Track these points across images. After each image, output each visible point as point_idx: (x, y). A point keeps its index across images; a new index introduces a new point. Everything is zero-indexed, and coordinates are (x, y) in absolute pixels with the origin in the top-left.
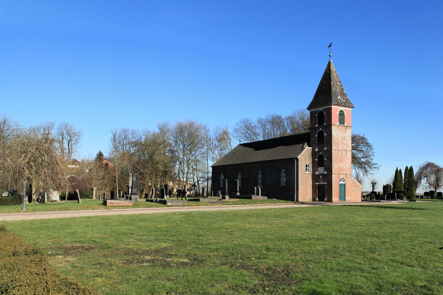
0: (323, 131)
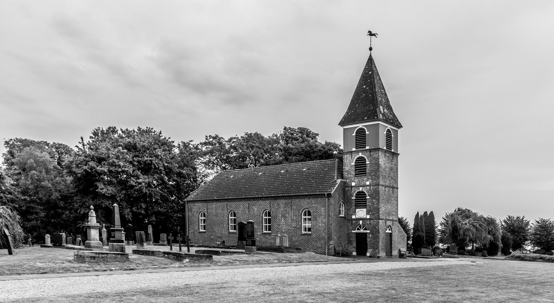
0: (365, 157)
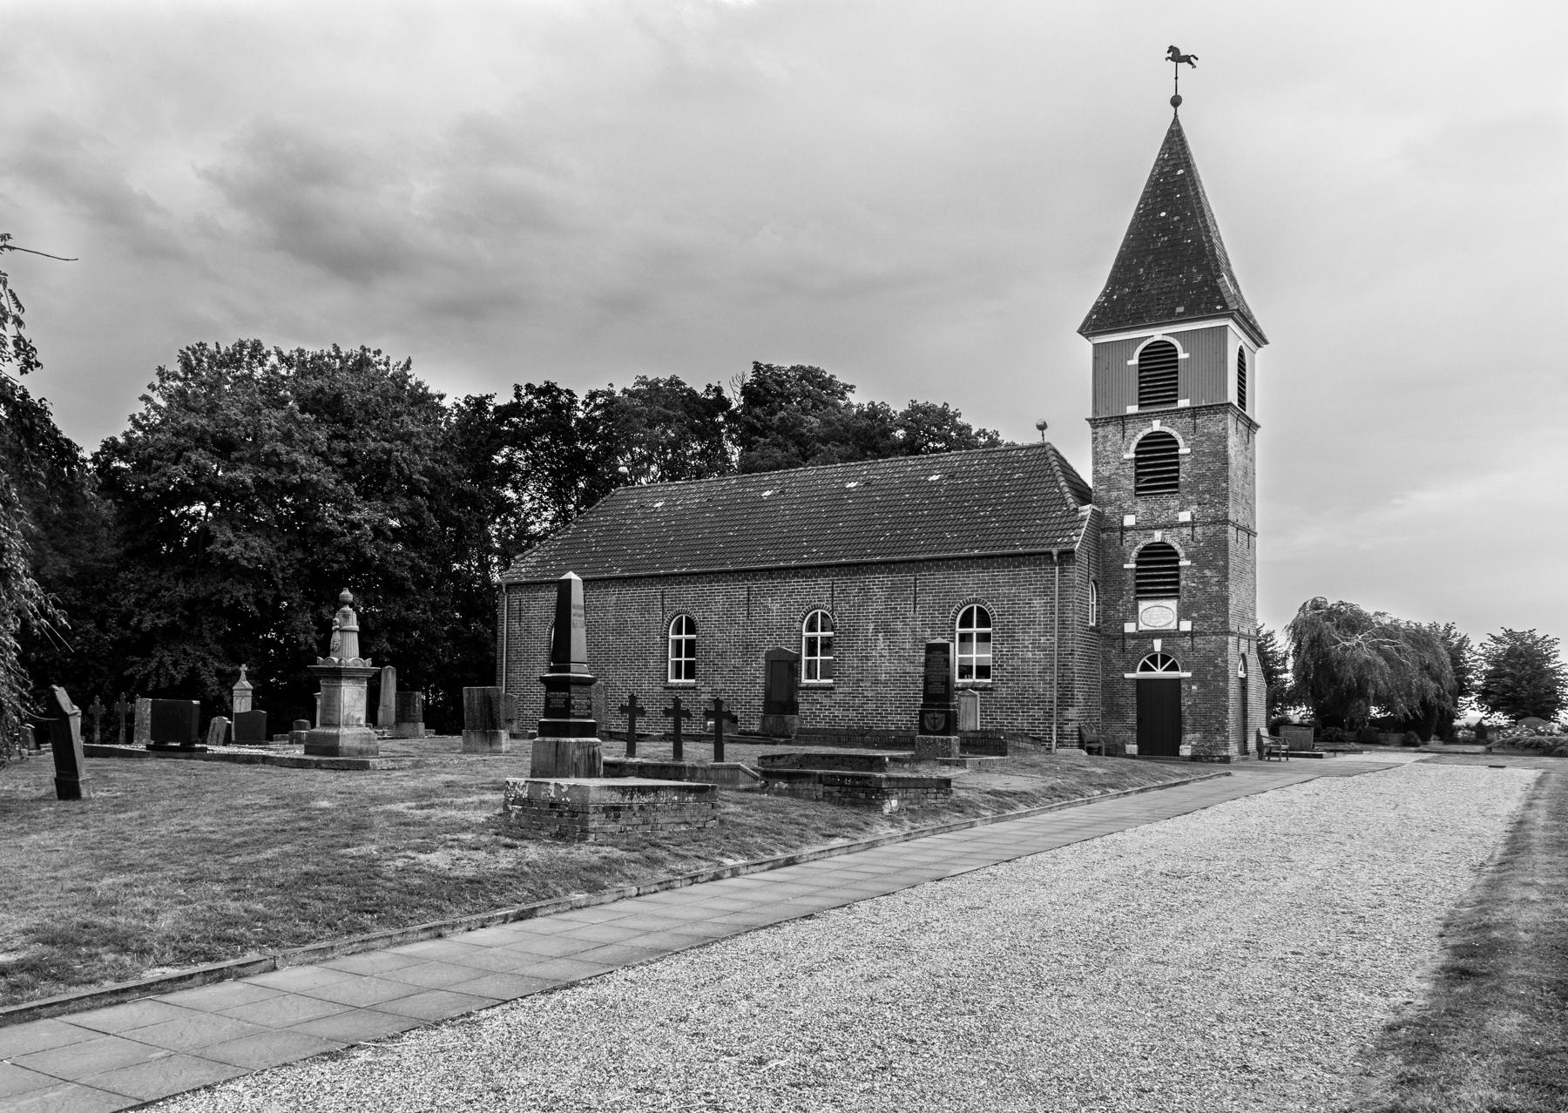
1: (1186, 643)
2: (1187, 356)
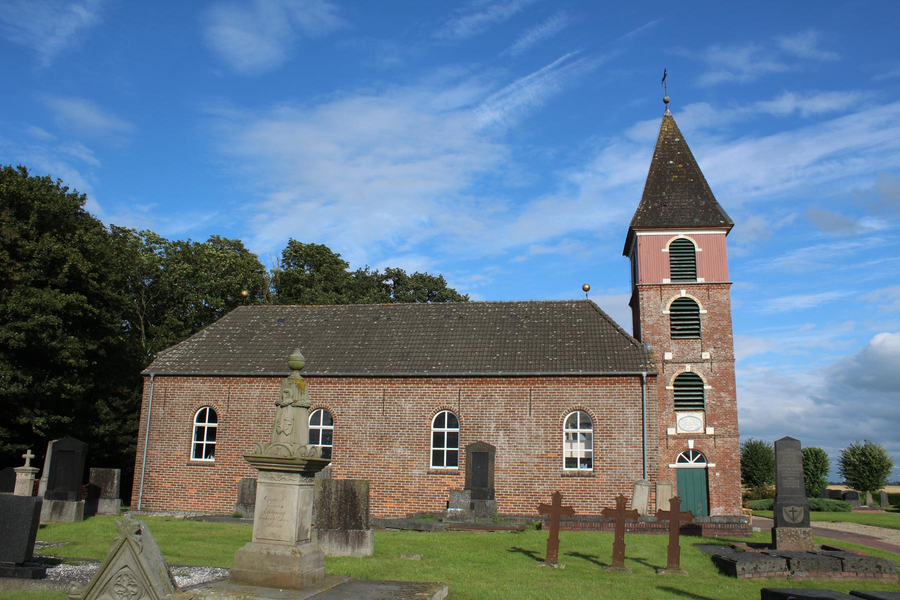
0: (695, 299)
1: (711, 443)
2: (701, 250)
